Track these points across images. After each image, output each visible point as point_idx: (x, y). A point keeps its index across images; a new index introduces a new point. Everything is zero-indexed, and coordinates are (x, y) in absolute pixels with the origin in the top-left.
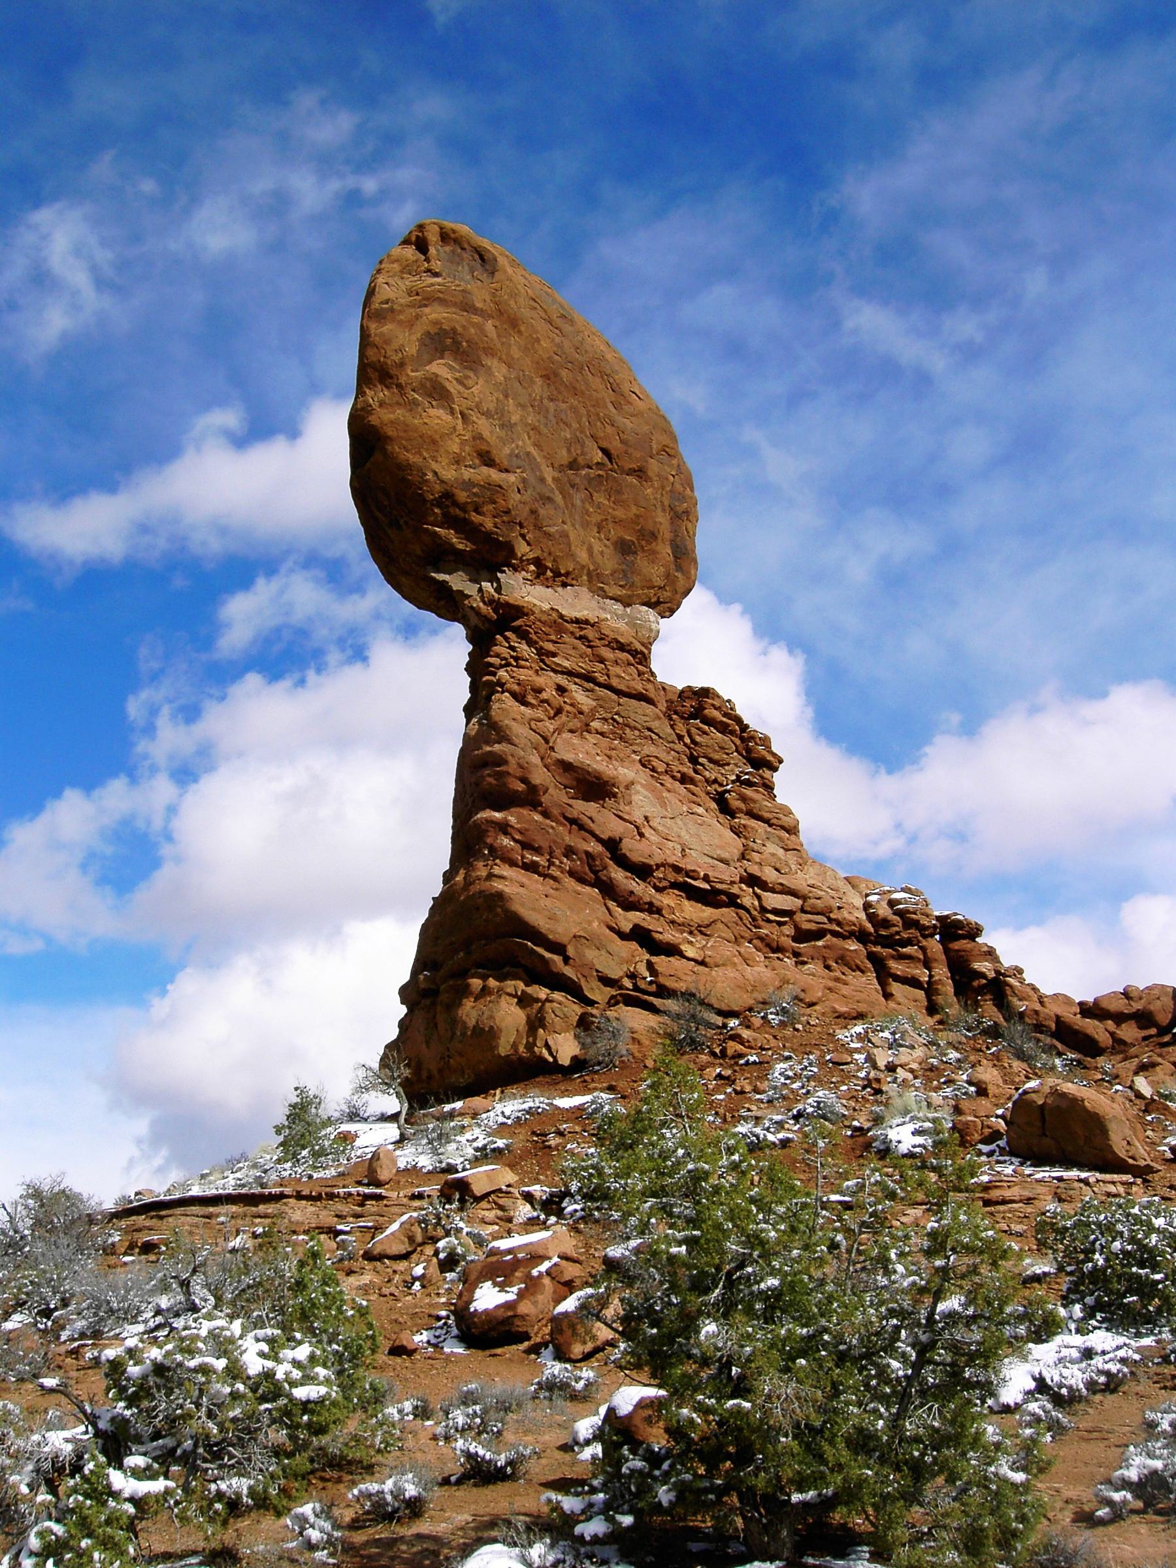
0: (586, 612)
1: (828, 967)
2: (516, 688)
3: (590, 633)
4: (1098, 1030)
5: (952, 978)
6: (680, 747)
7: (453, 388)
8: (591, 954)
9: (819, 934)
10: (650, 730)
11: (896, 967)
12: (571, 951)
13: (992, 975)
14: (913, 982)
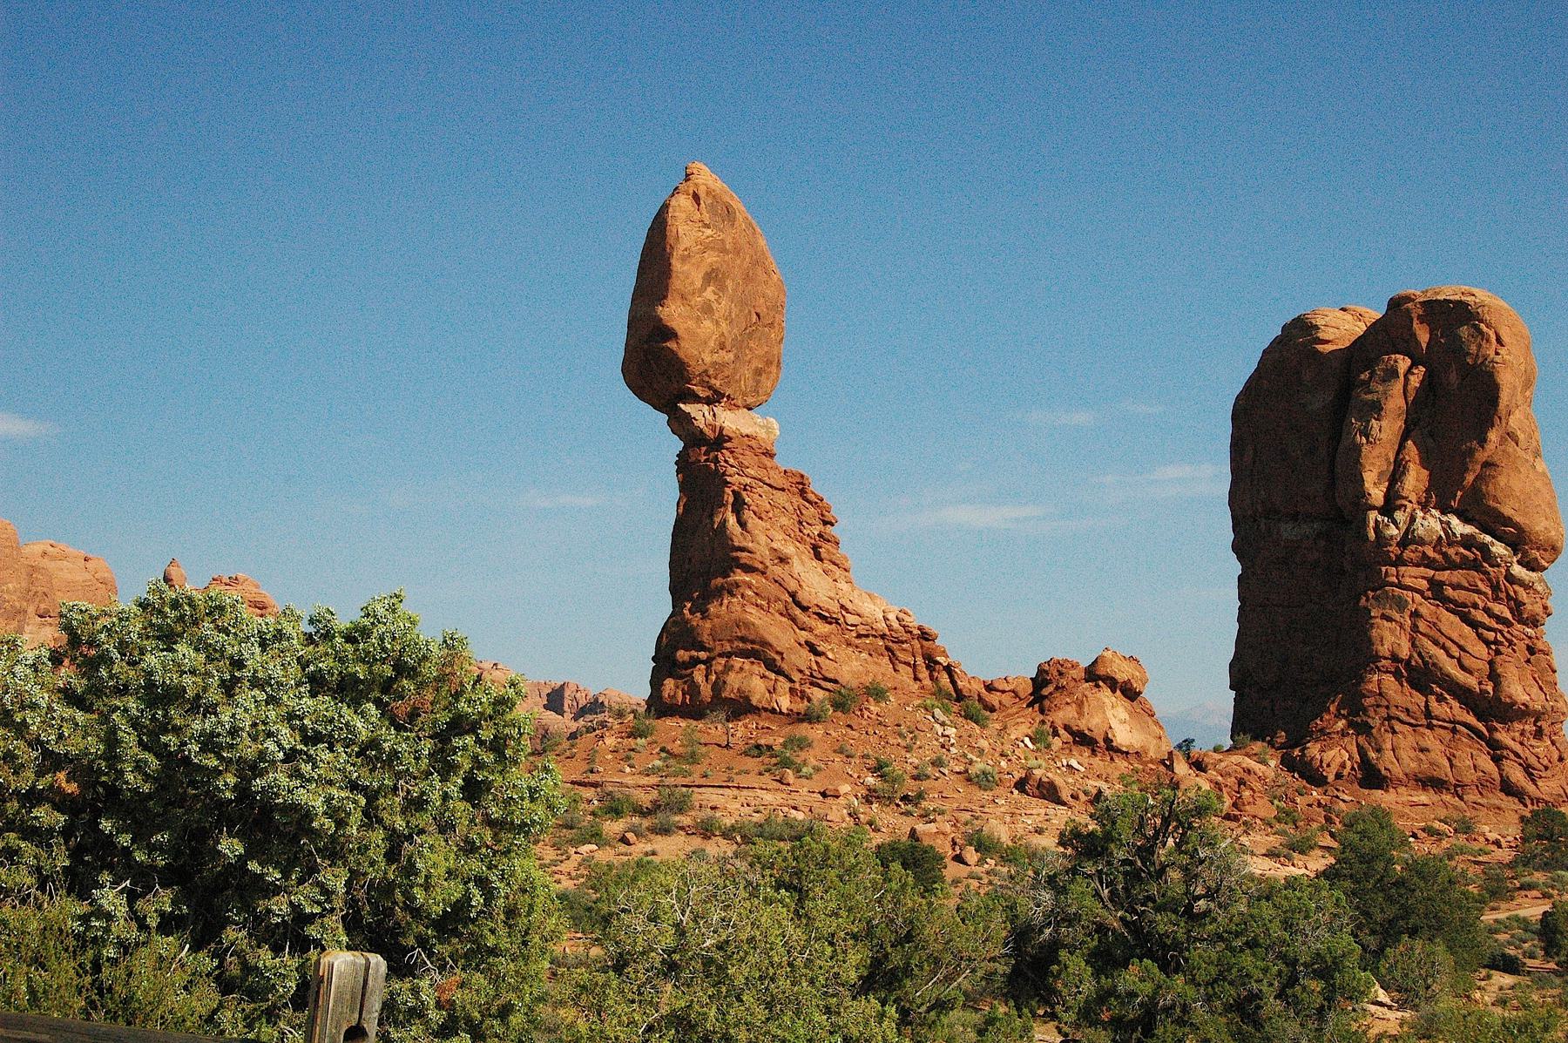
0: (750, 429)
1: (871, 655)
2: (755, 509)
3: (753, 443)
4: (994, 699)
5: (925, 663)
6: (795, 517)
7: (715, 306)
8: (793, 657)
9: (867, 636)
10: (784, 508)
11: (901, 656)
12: (784, 656)
13: (945, 664)
14: (908, 664)
